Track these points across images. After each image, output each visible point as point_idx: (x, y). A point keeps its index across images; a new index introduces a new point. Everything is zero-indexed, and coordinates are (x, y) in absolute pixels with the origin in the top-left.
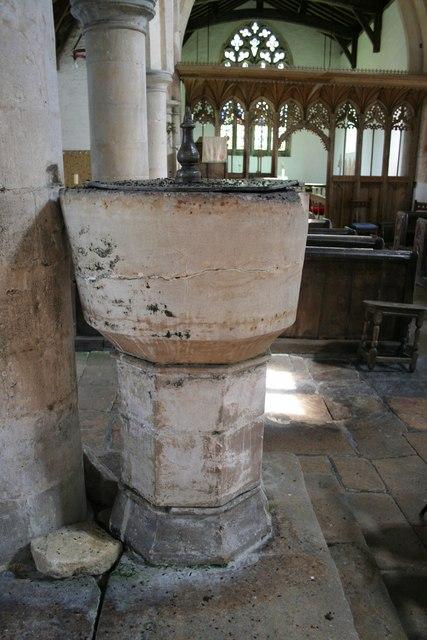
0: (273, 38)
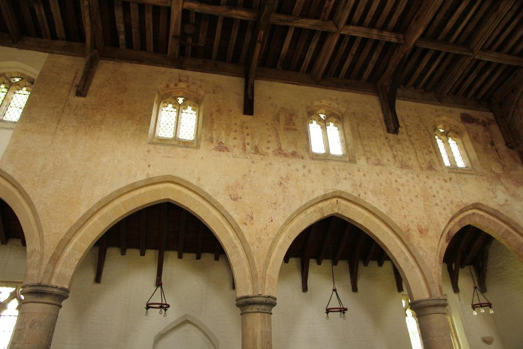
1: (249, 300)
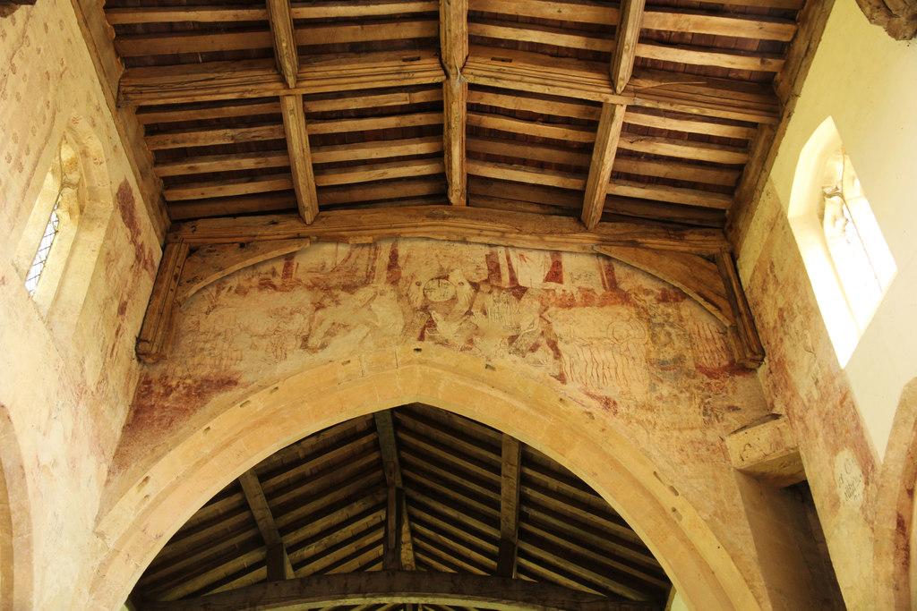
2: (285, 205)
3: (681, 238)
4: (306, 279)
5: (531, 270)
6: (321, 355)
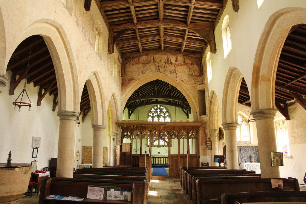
0: (164, 109)
1: (74, 114)
2: (138, 51)
3: (194, 55)
4: (142, 62)
5: (173, 59)
6: (145, 74)
